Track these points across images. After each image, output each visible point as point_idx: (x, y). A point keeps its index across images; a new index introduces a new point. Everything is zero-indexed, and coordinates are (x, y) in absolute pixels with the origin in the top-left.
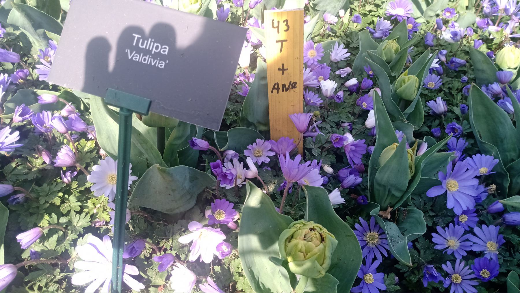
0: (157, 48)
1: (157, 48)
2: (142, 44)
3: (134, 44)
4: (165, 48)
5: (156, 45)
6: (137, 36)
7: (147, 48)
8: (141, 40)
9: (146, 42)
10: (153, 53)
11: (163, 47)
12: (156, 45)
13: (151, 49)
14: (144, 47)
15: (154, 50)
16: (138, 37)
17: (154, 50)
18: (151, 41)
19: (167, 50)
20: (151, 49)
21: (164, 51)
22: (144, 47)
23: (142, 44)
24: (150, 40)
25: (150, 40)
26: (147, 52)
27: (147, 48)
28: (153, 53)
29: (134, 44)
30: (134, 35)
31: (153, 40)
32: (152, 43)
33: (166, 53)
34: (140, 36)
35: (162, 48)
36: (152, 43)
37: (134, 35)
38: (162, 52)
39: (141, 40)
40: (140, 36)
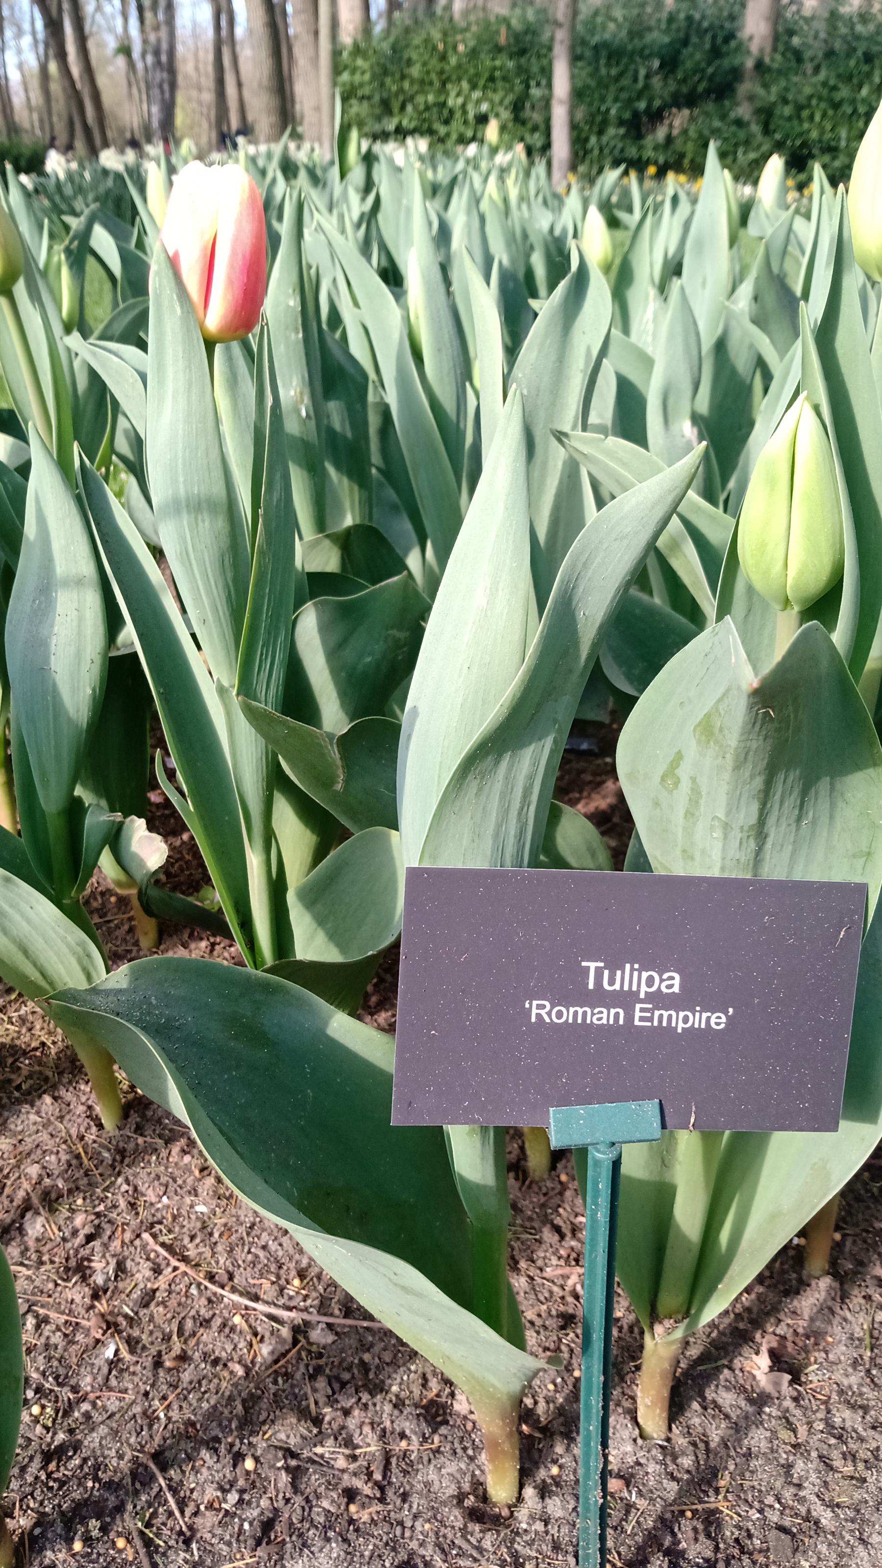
0: (650, 981)
1: (650, 981)
2: (612, 982)
3: (591, 986)
4: (672, 978)
6: (593, 965)
7: (626, 988)
8: (606, 972)
9: (619, 973)
10: (642, 996)
11: (665, 976)
13: (634, 988)
14: (617, 987)
15: (644, 988)
16: (597, 968)
17: (644, 988)
18: (632, 970)
19: (677, 982)
20: (634, 988)
21: (670, 987)
23: (612, 982)
24: (628, 966)
25: (628, 966)
26: (626, 999)
27: (626, 988)
28: (642, 996)
29: (591, 986)
30: (584, 964)
31: (636, 966)
32: (636, 974)
33: (676, 989)
34: (602, 964)
35: (662, 981)
36: (636, 974)
37: (584, 964)
38: (665, 990)
39: (606, 972)
40: (602, 964)
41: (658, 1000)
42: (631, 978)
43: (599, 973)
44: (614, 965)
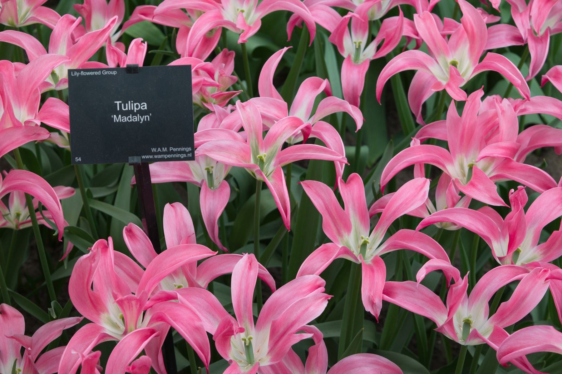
0: (137, 106)
1: (137, 106)
2: (125, 108)
3: (118, 109)
4: (144, 105)
5: (135, 104)
6: (118, 102)
12: (135, 104)
15: (135, 109)
18: (131, 103)
19: (146, 106)
22: (127, 109)
23: (125, 108)
29: (118, 109)
33: (146, 108)
35: (141, 106)
41: (141, 113)
42: (131, 106)
43: (120, 104)
44: (125, 102)
